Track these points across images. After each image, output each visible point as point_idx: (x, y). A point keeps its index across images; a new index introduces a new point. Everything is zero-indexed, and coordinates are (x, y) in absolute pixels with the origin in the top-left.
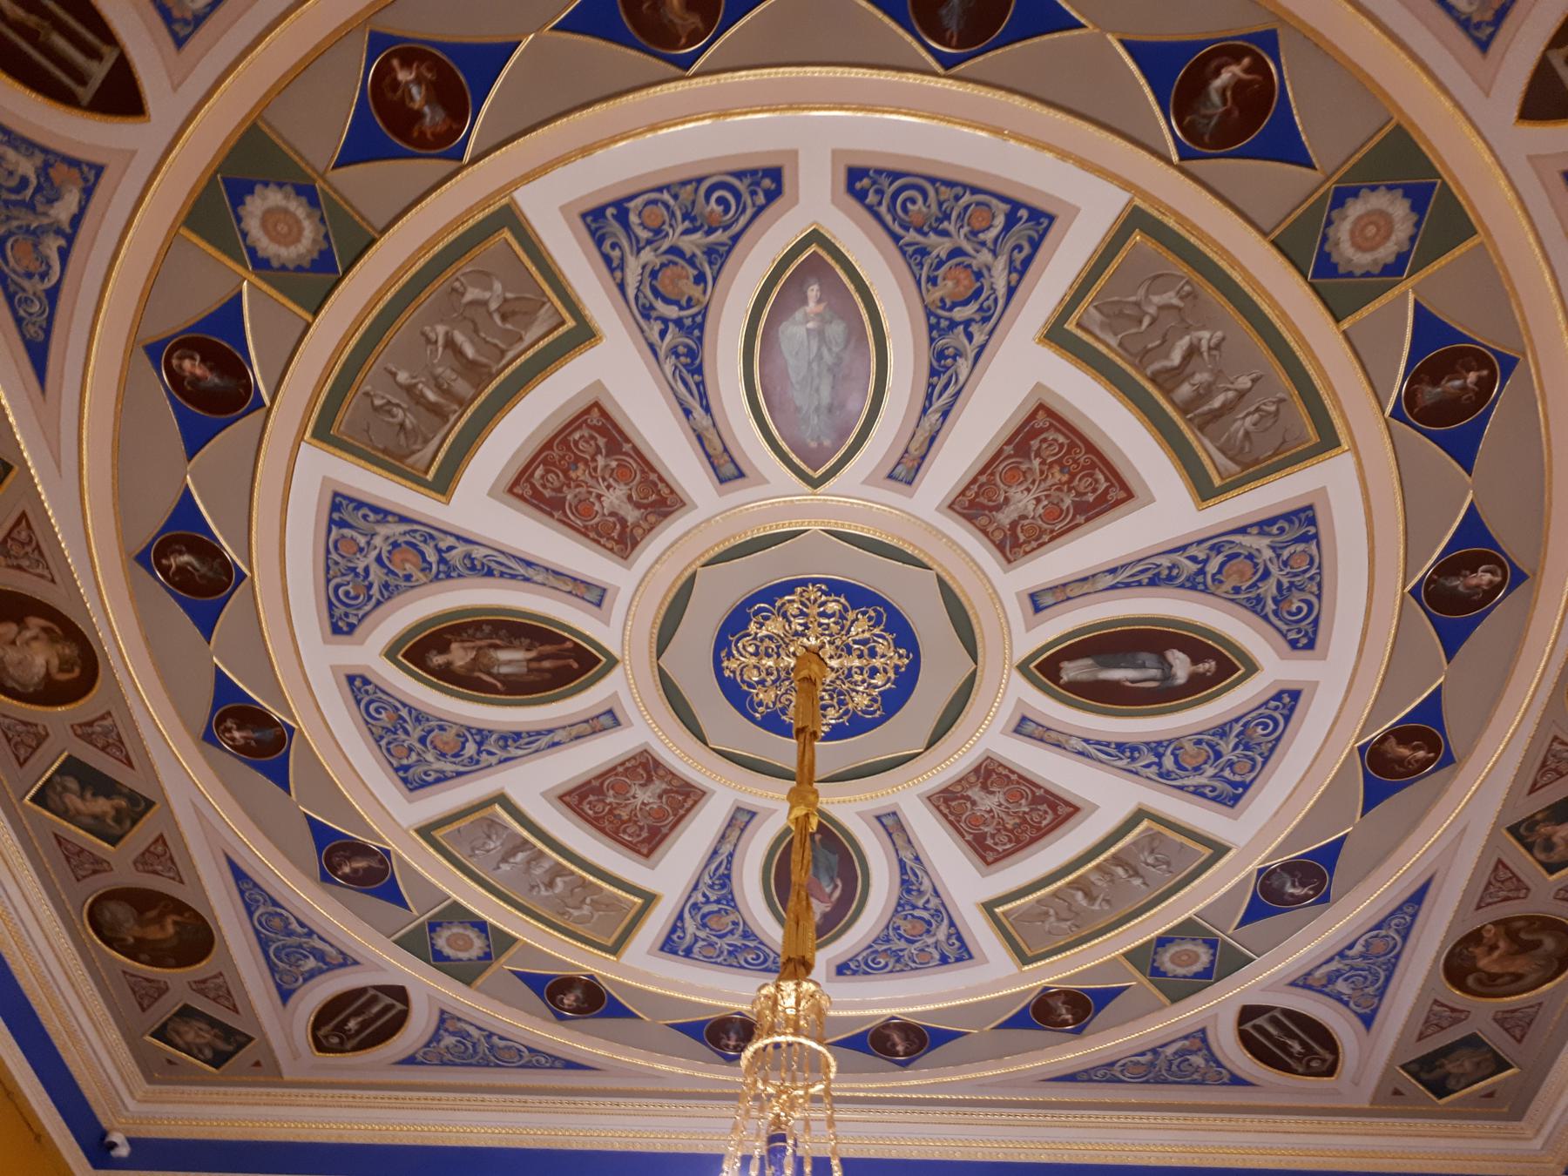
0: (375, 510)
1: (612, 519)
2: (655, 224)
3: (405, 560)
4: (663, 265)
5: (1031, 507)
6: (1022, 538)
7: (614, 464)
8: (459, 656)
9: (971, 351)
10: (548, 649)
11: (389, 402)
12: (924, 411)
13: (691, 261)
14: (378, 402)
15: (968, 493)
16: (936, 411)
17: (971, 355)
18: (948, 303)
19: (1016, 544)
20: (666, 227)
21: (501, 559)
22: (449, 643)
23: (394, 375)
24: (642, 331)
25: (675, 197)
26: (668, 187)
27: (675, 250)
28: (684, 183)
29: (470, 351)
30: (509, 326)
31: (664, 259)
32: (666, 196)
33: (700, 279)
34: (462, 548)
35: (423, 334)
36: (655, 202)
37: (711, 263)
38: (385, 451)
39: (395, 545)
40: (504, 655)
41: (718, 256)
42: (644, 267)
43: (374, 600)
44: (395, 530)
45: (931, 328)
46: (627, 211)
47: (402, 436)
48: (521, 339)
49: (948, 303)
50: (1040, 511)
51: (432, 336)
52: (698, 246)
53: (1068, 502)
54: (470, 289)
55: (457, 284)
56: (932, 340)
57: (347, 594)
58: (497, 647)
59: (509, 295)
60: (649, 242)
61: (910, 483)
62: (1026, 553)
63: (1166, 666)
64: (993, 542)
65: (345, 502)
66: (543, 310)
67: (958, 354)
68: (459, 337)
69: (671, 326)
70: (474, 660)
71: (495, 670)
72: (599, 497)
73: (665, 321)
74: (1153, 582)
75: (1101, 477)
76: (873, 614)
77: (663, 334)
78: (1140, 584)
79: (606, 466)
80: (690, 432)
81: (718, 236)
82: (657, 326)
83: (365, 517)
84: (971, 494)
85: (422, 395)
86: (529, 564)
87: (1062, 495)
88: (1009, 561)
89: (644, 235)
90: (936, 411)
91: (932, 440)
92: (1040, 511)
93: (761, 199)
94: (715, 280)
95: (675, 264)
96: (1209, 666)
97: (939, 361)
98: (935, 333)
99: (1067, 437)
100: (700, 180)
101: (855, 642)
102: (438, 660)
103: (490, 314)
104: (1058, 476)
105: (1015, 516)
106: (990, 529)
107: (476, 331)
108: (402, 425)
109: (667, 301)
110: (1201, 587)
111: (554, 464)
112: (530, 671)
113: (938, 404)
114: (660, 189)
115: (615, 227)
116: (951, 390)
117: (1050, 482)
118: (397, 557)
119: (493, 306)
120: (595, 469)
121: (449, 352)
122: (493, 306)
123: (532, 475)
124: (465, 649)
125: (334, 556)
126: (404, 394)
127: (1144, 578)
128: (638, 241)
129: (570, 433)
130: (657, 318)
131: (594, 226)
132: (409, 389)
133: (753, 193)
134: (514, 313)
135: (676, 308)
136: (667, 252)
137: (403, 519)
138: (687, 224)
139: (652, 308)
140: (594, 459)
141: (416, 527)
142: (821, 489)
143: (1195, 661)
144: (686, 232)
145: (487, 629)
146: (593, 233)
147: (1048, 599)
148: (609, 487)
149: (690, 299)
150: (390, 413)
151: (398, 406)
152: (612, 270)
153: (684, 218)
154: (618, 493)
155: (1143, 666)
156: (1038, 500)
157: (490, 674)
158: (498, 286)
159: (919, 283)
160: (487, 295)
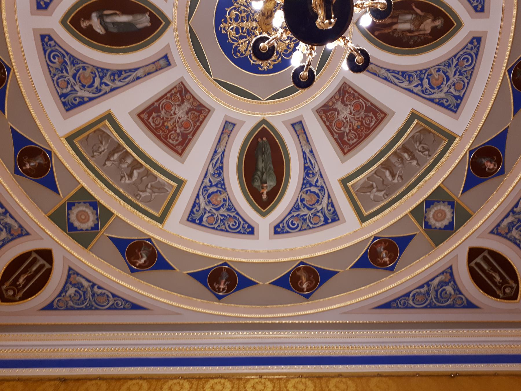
0: (442, 105)
1: (347, 103)
2: (315, 217)
3: (437, 80)
4: (314, 204)
5: (177, 110)
6: (178, 95)
7: (342, 129)
8: (428, 25)
9: (209, 176)
10: (386, 31)
11: (422, 152)
12: (223, 153)
13: (305, 206)
14: (427, 153)
16: (219, 153)
17: (209, 174)
18: (219, 192)
19: (180, 92)
20: (312, 216)
21: (396, 81)
22: (430, 34)
23: (418, 164)
24: (324, 182)
25: (308, 225)
26: (310, 228)
27: (310, 209)
28: (305, 229)
29: (387, 173)
30: (371, 183)
31: (314, 206)
32: (311, 226)
33: (302, 200)
34: (411, 87)
35: (402, 179)
36: (315, 224)
37: (298, 205)
38: (430, 132)
39: (439, 88)
40: (407, 26)
41: (296, 208)
42: (321, 203)
43: (457, 57)
44: (438, 95)
45: (224, 184)
46: (324, 221)
47: (422, 138)
48: (368, 178)
49: (219, 192)
50: (173, 108)
51: (399, 178)
52: (302, 211)
53: (163, 112)
54: (382, 195)
55: (386, 197)
56: (223, 180)
57: (467, 61)
58: (410, 31)
59: (369, 194)
60: (318, 212)
62: (175, 87)
63: (103, 24)
64: (190, 93)
65: (453, 108)
66: (358, 188)
67: (213, 175)
68: (390, 178)
69: (314, 184)
70: (422, 23)
71: (414, 16)
72: (351, 114)
73: (316, 186)
74: (120, 72)
75: (152, 124)
76: (238, 54)
77: (317, 181)
78: (125, 71)
79: (345, 128)
80: (311, 144)
81: (295, 214)
82: (319, 184)
83: (447, 101)
84: (202, 117)
85: (409, 155)
86: (386, 79)
87: (166, 116)
88: (182, 83)
89: (320, 214)
90: (219, 153)
91: (219, 141)
92: (173, 108)
93: (281, 225)
94: (297, 200)
95: (310, 205)
96: (84, 24)
97: (220, 172)
98: (222, 182)
99: (168, 141)
100: (300, 230)
101: (245, 37)
102: (438, 23)
103: (377, 187)
104: (169, 124)
105: (183, 106)
106: (192, 100)
107: (383, 181)
108: (420, 143)
109: (314, 193)
110: (100, 70)
111: (366, 128)
112: (397, 17)
113: (218, 156)
114: (313, 228)
115: (328, 216)
116: (214, 161)
117: (172, 122)
118: (439, 82)
119: (375, 190)
120: (350, 126)
121: (395, 172)
122: (375, 190)
123: (376, 122)
124: (425, 30)
125: (466, 81)
126: (416, 156)
127: (124, 75)
128: (322, 212)
129: (357, 141)
130: (319, 186)
131: (336, 216)
132: (413, 158)
133: (283, 227)
134: (368, 187)
135: (312, 190)
136: (312, 209)
137: (432, 100)
138: (305, 217)
139: (320, 190)
140: (350, 130)
141: (428, 97)
142: (261, 119)
143: (91, 27)
144: (306, 215)
145: (412, 42)
146: (336, 214)
147: (162, 62)
148: (346, 118)
149: (307, 193)
150: (423, 147)
151: (420, 151)
152: (332, 203)
153: (306, 219)
154: (343, 116)
155: (114, 24)
156: (175, 114)
157: (417, 14)
158: (372, 197)
159: (229, 199)
160: (376, 194)
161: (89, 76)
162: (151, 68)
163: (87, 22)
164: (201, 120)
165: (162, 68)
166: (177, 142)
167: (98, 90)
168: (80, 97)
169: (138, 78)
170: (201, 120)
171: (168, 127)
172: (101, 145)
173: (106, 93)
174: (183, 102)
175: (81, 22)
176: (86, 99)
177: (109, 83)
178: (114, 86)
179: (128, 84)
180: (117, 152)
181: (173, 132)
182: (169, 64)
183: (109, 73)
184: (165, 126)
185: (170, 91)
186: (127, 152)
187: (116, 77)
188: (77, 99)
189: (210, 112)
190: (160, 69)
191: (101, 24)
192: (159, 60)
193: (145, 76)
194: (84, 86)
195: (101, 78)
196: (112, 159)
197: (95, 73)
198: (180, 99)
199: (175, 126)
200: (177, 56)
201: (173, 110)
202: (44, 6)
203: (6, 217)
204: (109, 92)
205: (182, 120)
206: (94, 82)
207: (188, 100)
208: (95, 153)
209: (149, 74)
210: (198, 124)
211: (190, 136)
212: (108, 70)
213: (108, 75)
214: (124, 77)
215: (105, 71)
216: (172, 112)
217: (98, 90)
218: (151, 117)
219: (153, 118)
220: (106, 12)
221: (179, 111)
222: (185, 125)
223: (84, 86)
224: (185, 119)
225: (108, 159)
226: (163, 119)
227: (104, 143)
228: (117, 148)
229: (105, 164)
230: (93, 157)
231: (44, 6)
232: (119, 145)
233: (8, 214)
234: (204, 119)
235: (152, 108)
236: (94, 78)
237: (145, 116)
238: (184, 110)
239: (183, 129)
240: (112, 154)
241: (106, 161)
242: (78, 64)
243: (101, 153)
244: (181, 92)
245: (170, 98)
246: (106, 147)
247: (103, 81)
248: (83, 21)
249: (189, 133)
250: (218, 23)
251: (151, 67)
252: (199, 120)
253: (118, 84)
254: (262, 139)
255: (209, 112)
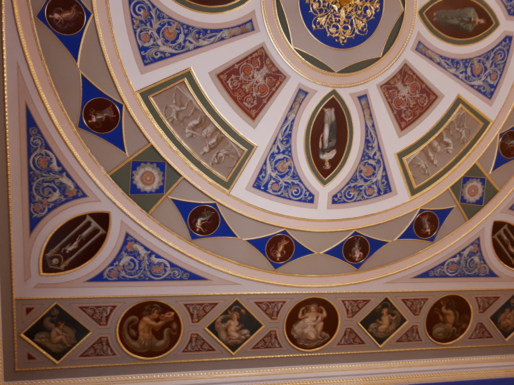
5: (402, 94)
6: (390, 91)
15: (410, 71)
19: (388, 89)
50: (400, 98)
53: (402, 107)
61: (416, 49)
62: (384, 93)
63: (329, 150)
74: (367, 141)
78: (367, 136)
84: (409, 72)
88: (381, 86)
105: (399, 88)
106: (395, 79)
110: (363, 159)
117: (411, 101)
127: (369, 138)
147: (363, 102)
156: (404, 97)
161: (367, 168)
162: (367, 113)
163: (326, 164)
164: (412, 74)
165: (368, 103)
166: (427, 98)
167: (378, 162)
168: (382, 179)
169: (373, 126)
170: (412, 74)
171: (414, 105)
172: (421, 166)
173: (381, 156)
174: (396, 88)
175: (326, 168)
176: (384, 174)
177: (374, 152)
178: (377, 148)
179: (376, 135)
180: (428, 153)
181: (418, 101)
182: (365, 96)
183: (367, 151)
184: (413, 108)
185: (387, 98)
186: (429, 145)
187: (370, 145)
188: (383, 181)
189: (407, 63)
190: (369, 105)
191: (328, 152)
192: (361, 105)
193: (372, 119)
194: (374, 174)
195: (369, 158)
196: (432, 158)
197: (365, 163)
198: (394, 90)
199: (414, 98)
200: (359, 90)
201: (402, 98)
202: (311, 197)
203: (463, 254)
204: (381, 152)
205: (410, 92)
206: (372, 165)
207: (395, 82)
208: (426, 172)
209: (371, 115)
210: (415, 77)
211: (424, 86)
212: (364, 152)
213: (368, 152)
214: (371, 140)
215: (365, 154)
216: (403, 99)
217: (378, 162)
218: (405, 118)
219: (406, 117)
220: (320, 146)
221: (402, 92)
222: (414, 88)
223: (374, 174)
224: (409, 88)
225: (432, 162)
226: (407, 108)
227: (420, 164)
228: (425, 152)
229: (436, 165)
230: (428, 175)
231: (311, 197)
232: (423, 150)
233: (462, 253)
234: (412, 71)
235: (398, 117)
236: (369, 164)
237: (403, 124)
238: (403, 87)
239: (417, 91)
240: (428, 158)
241: (433, 164)
242: (356, 176)
243: (427, 167)
244: (388, 88)
245: (392, 99)
246: (423, 162)
247: (372, 157)
248: (325, 167)
249: (421, 86)
250: (338, 45)
251: (366, 113)
252: (412, 76)
253: (375, 144)
254: (434, 17)
255: (407, 66)
